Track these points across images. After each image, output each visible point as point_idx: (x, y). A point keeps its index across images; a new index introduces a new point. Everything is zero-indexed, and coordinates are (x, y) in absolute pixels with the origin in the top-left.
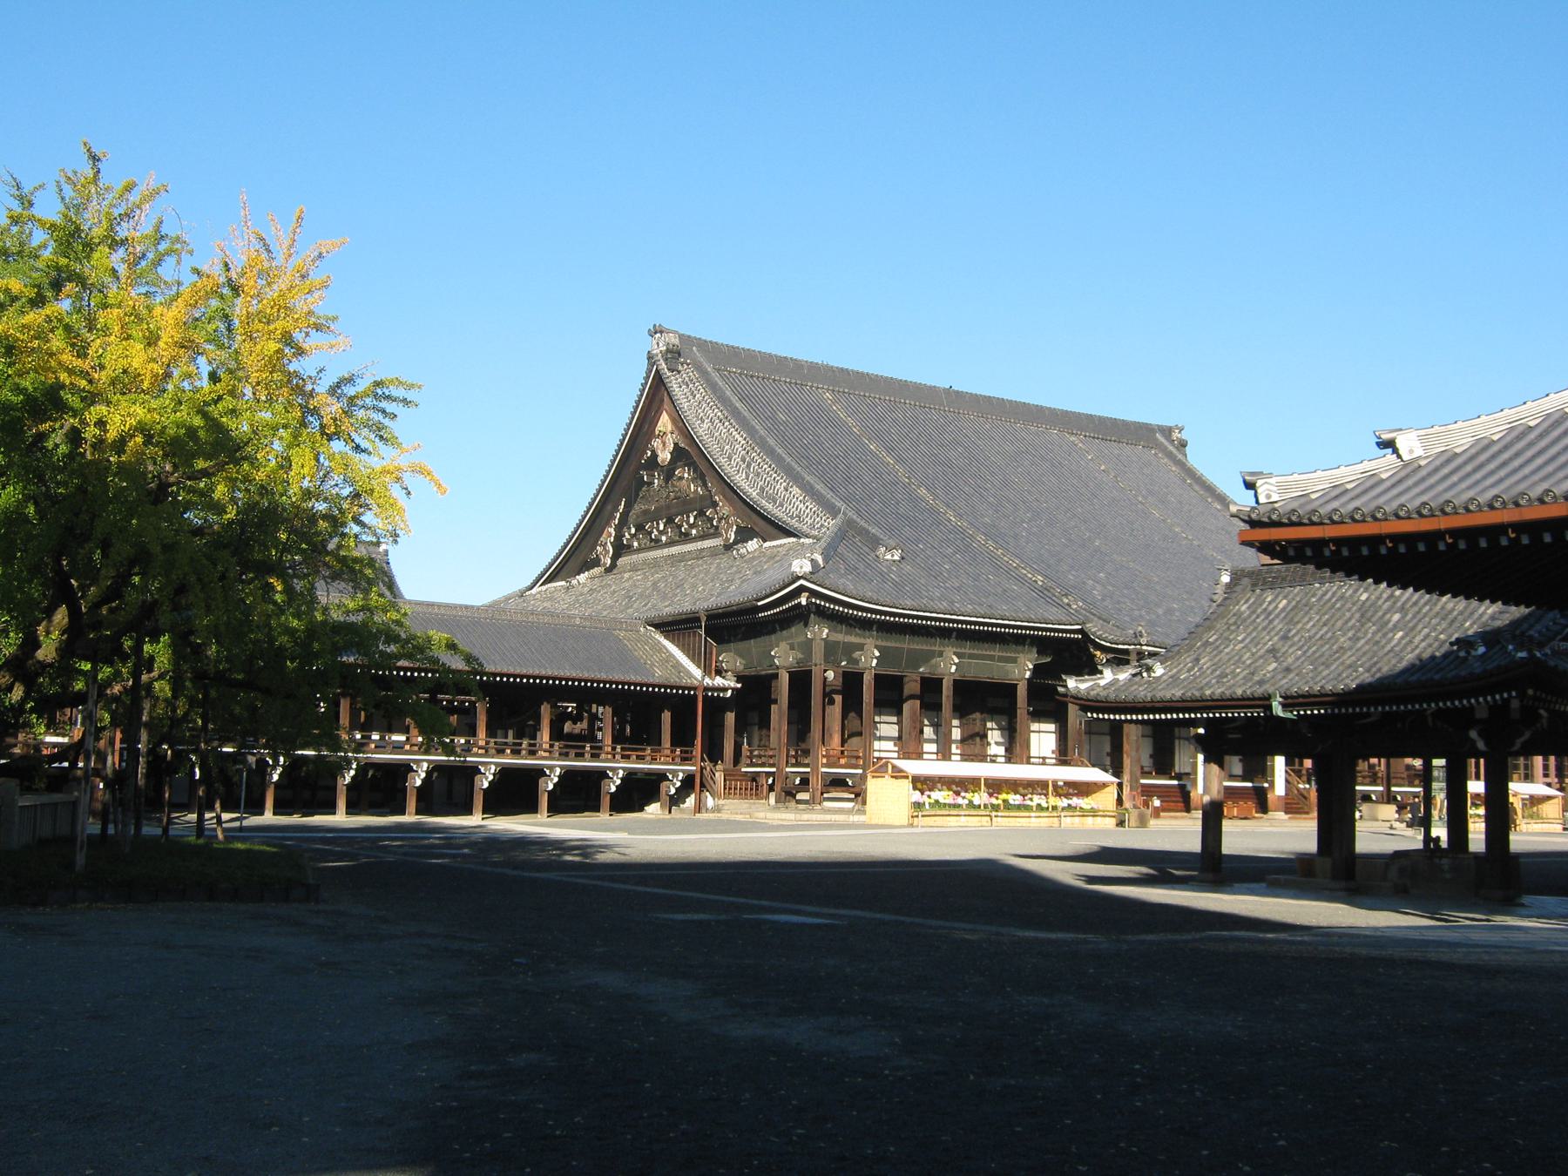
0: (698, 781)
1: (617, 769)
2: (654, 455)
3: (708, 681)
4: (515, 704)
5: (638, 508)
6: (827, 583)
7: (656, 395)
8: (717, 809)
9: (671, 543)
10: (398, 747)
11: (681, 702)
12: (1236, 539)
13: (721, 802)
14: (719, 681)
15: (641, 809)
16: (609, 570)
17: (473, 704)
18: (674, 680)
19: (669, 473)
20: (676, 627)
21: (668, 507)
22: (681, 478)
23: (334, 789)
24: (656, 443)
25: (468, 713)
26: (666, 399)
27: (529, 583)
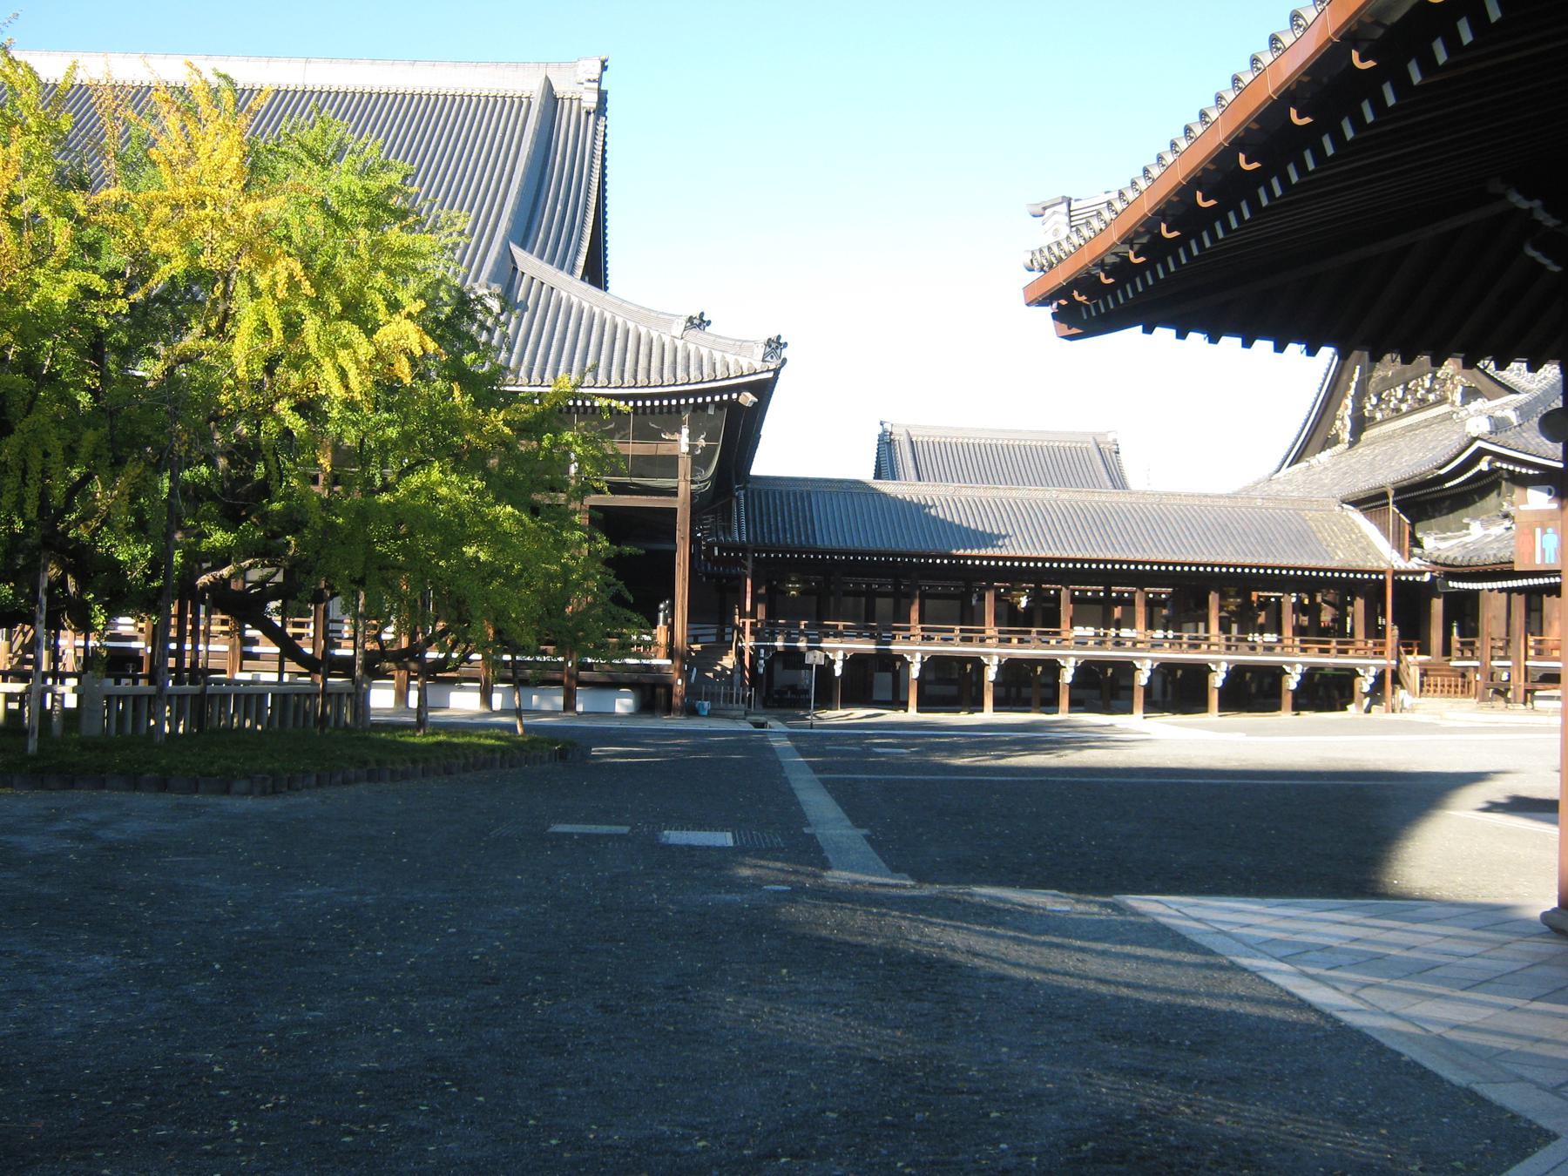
0: (1389, 676)
1: (1296, 662)
3: (1400, 563)
4: (1185, 593)
6: (1512, 442)
8: (1412, 710)
9: (1412, 411)
13: (1417, 700)
15: (1344, 709)
16: (1352, 445)
17: (1058, 592)
18: (1358, 563)
20: (1369, 503)
25: (1129, 603)
27: (1276, 467)
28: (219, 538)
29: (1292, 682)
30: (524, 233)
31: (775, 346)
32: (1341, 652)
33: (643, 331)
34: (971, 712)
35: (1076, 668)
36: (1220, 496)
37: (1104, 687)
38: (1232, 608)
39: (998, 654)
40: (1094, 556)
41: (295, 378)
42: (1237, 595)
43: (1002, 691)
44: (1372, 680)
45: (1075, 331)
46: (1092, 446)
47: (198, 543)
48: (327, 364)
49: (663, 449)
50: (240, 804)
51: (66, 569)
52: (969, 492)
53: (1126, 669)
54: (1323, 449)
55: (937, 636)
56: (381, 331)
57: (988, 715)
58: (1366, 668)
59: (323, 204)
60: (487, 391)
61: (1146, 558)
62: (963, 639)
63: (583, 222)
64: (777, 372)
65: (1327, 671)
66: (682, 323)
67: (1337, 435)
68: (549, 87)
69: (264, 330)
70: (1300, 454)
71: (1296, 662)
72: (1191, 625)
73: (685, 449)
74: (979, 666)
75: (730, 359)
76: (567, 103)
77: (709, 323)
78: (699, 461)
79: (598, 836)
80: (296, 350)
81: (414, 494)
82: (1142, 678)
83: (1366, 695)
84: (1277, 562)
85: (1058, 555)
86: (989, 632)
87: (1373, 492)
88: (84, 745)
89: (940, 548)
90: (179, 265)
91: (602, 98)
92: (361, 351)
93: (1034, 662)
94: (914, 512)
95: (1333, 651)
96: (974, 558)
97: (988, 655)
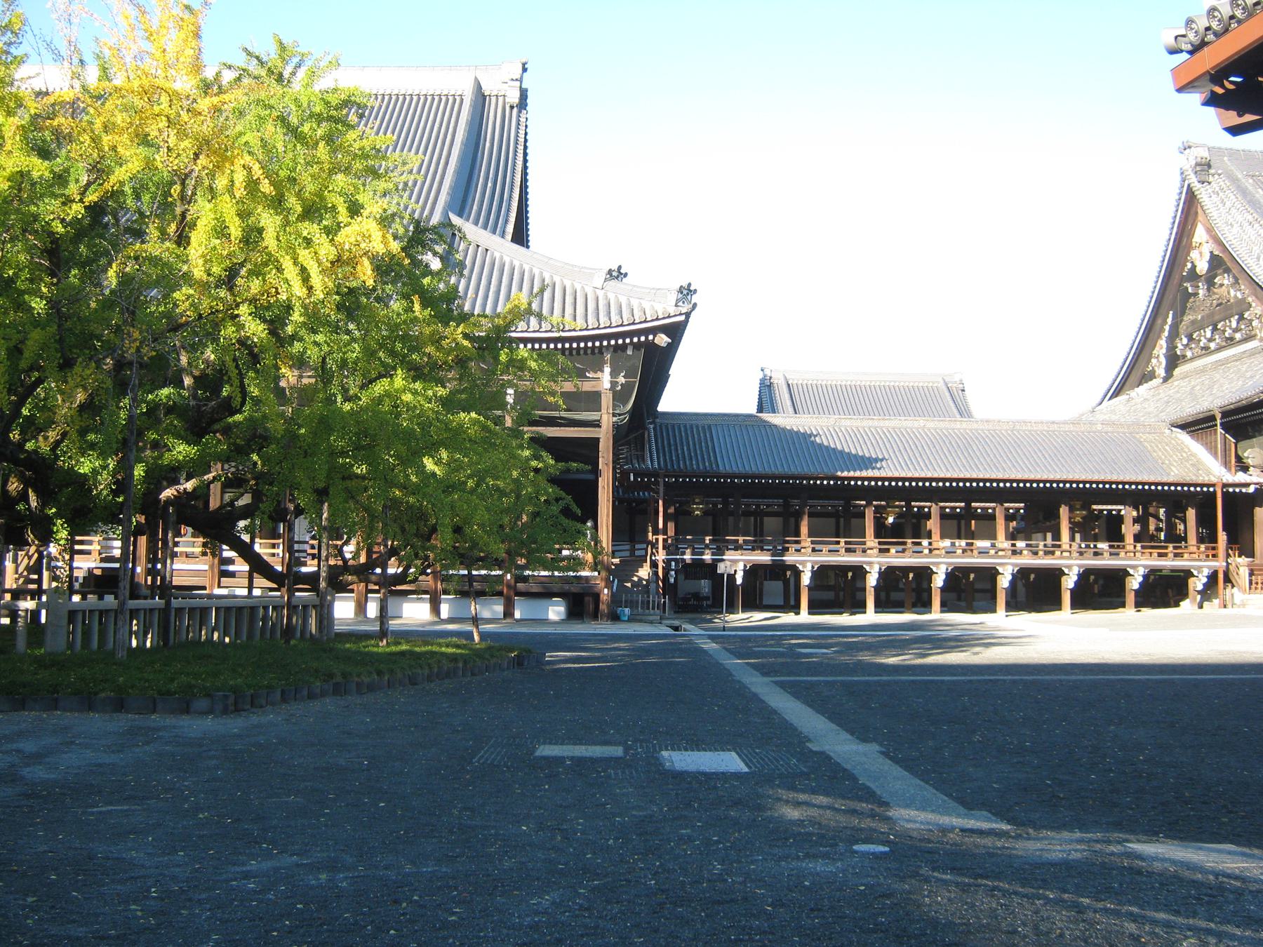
0: (1221, 576)
2: (1194, 267)
3: (1229, 477)
4: (1038, 507)
5: (1188, 318)
7: (1190, 206)
8: (1243, 605)
9: (1220, 349)
10: (983, 553)
11: (1200, 500)
12: (1170, 87)
13: (1247, 596)
14: (1241, 477)
15: (1177, 605)
16: (1166, 380)
18: (1191, 477)
19: (1210, 282)
20: (1197, 426)
21: (1212, 314)
22: (1222, 285)
23: (864, 589)
24: (1194, 255)
26: (1200, 211)
28: (182, 450)
29: (1134, 583)
30: (461, 203)
31: (686, 292)
32: (1176, 555)
33: (568, 284)
34: (853, 614)
35: (947, 574)
36: (1065, 423)
37: (970, 589)
38: (1078, 519)
39: (879, 563)
40: (962, 476)
41: (255, 286)
42: (1083, 508)
43: (883, 595)
44: (1205, 580)
45: (1249, 118)
46: (941, 385)
47: (161, 456)
48: (287, 263)
49: (587, 387)
50: (198, 726)
51: (27, 483)
52: (848, 423)
53: (991, 574)
54: (1140, 384)
55: (825, 548)
56: (343, 232)
57: (870, 617)
58: (1199, 569)
59: (283, 120)
60: (445, 307)
61: (1006, 477)
62: (848, 550)
63: (510, 197)
64: (688, 315)
65: (1164, 573)
66: (603, 275)
67: (1153, 372)
68: (478, 87)
69: (221, 231)
70: (1118, 390)
71: (1138, 564)
72: (1040, 535)
73: (607, 385)
74: (860, 572)
75: (647, 306)
76: (494, 99)
77: (626, 275)
78: (619, 396)
79: (593, 761)
80: (257, 258)
81: (379, 400)
82: (1004, 582)
83: (1199, 592)
84: (1121, 478)
85: (929, 475)
86: (869, 544)
87: (1201, 416)
88: (55, 663)
89: (826, 471)
90: (134, 166)
91: (524, 94)
92: (322, 252)
93: (905, 570)
94: (802, 441)
95: (1171, 555)
96: (856, 479)
97: (870, 563)
